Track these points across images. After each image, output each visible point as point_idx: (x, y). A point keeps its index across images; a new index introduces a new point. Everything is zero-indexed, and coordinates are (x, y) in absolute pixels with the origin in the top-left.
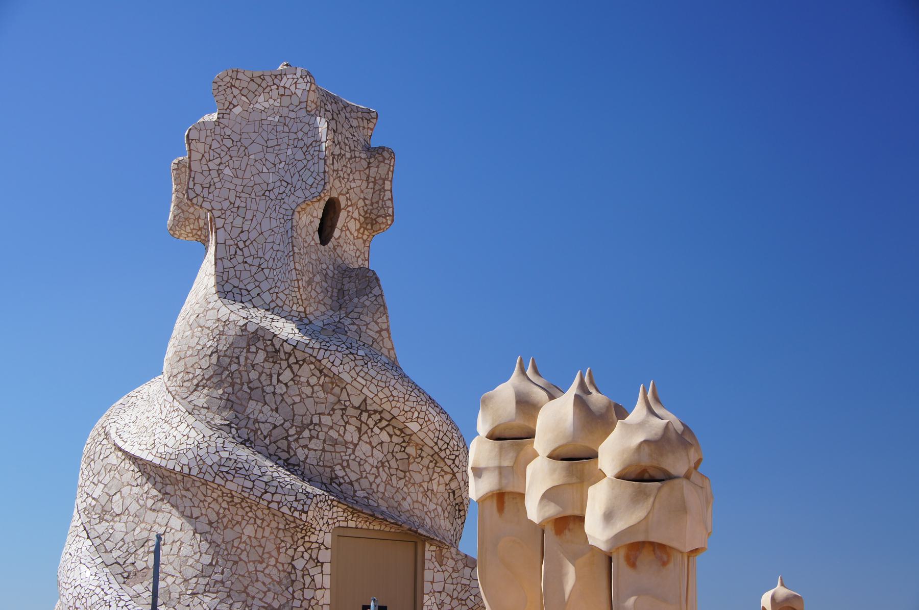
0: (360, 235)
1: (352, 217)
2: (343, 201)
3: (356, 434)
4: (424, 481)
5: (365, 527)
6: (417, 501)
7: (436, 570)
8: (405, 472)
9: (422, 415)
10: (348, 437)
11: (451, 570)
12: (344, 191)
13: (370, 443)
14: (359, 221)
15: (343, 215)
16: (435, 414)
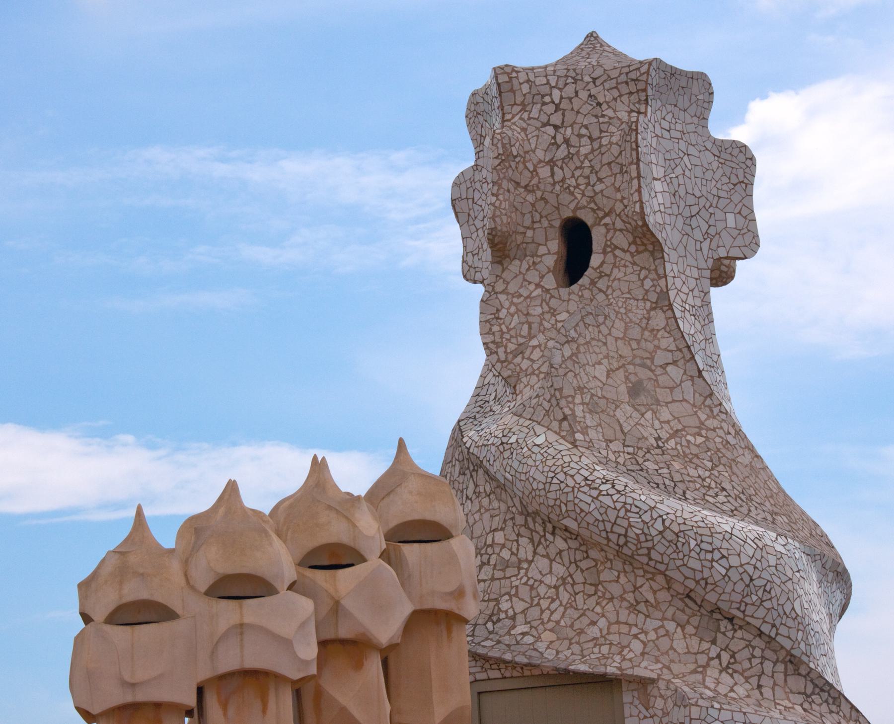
0: (641, 248)
1: (615, 230)
2: (588, 218)
3: (530, 548)
4: (625, 592)
5: (515, 674)
6: (618, 622)
7: (641, 716)
8: (596, 585)
9: (570, 506)
10: (522, 555)
11: (660, 713)
12: (584, 202)
13: (547, 556)
14: (627, 230)
15: (598, 236)
16: (589, 500)
